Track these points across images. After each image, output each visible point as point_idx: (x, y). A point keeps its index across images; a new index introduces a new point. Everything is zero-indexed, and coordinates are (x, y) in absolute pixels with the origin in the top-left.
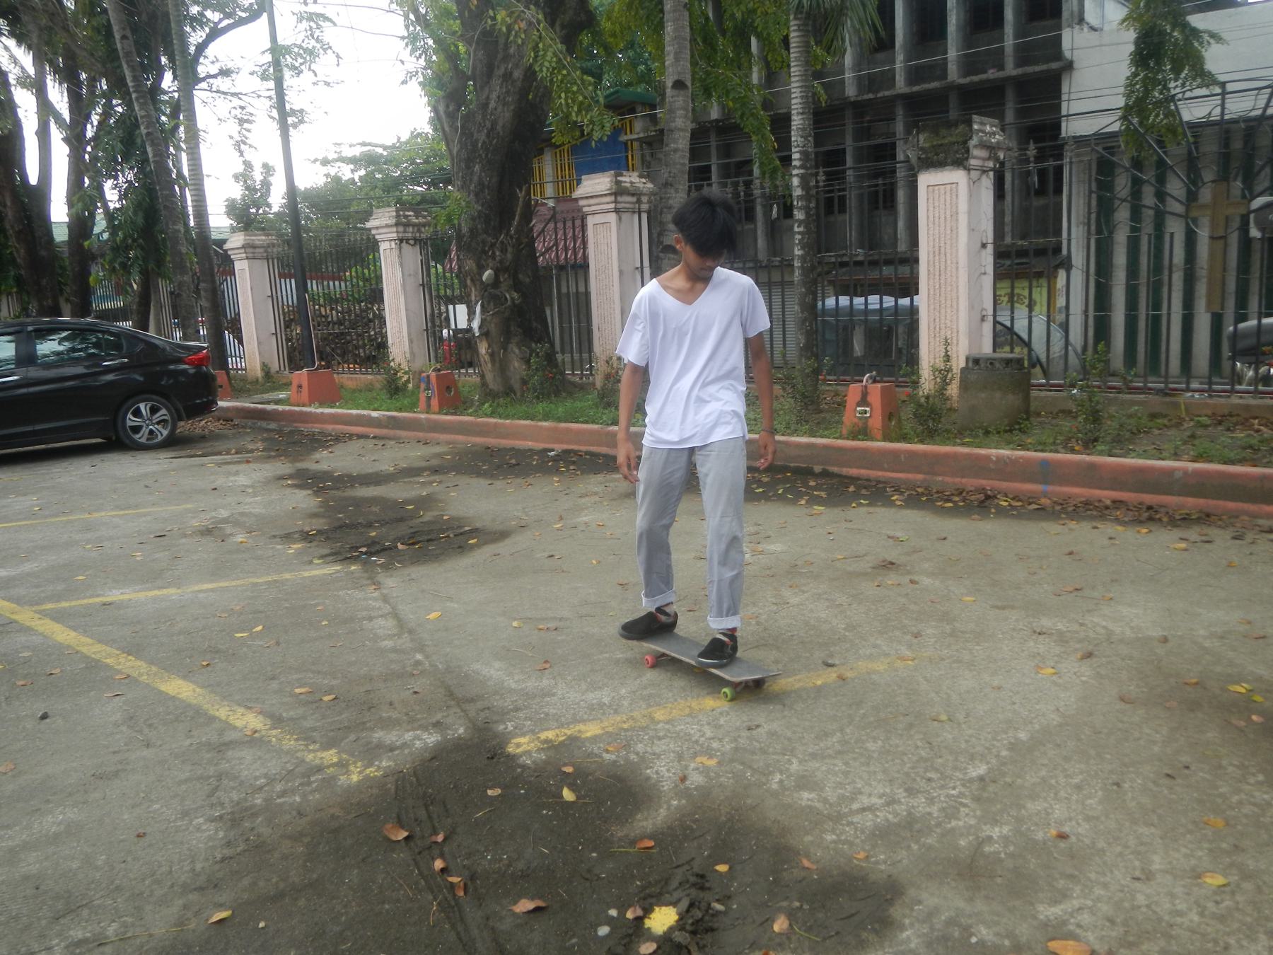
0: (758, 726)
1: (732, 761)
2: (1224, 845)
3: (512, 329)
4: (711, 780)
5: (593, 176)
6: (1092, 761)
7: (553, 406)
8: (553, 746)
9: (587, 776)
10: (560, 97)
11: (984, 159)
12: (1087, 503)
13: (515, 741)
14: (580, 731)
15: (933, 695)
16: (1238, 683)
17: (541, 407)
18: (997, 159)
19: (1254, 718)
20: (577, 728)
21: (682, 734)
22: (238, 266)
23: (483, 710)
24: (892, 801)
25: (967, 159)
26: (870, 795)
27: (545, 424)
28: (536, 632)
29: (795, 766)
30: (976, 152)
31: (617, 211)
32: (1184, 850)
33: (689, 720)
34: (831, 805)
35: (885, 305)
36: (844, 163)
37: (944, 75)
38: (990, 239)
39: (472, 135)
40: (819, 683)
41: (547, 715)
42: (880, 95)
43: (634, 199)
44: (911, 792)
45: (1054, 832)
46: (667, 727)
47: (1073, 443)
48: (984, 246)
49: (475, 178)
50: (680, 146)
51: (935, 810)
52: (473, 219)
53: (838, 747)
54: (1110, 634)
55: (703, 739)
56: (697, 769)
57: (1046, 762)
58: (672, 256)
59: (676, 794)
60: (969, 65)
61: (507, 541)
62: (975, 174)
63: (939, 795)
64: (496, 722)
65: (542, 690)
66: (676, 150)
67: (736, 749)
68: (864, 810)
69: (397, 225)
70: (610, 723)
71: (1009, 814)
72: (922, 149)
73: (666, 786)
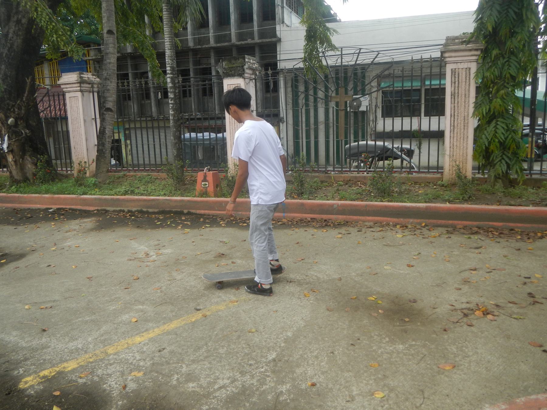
0: (164, 349)
1: (151, 371)
2: (380, 376)
3: (26, 148)
4: (140, 385)
5: (68, 73)
6: (320, 343)
7: (51, 187)
8: (48, 379)
9: (69, 396)
11: (251, 74)
12: (301, 220)
13: (24, 380)
14: (64, 368)
15: (248, 319)
16: (371, 296)
17: (44, 187)
19: (380, 311)
20: (63, 366)
21: (123, 360)
23: (4, 363)
24: (234, 381)
25: (244, 74)
26: (223, 379)
28: (39, 310)
29: (184, 369)
30: (247, 71)
31: (81, 91)
32: (364, 382)
33: (127, 351)
34: (204, 388)
35: (211, 137)
36: (189, 75)
37: (230, 40)
40: (193, 320)
41: (45, 360)
42: (204, 46)
43: (90, 86)
44: (243, 373)
45: (310, 384)
46: (115, 357)
47: (293, 195)
49: (2, 72)
50: (112, 61)
51: (254, 381)
53: (205, 354)
54: (318, 279)
55: (135, 361)
56: (133, 379)
57: (301, 346)
59: (121, 397)
60: (240, 36)
61: (24, 260)
62: (247, 80)
63: (256, 373)
64: (13, 369)
65: (42, 345)
66: (110, 63)
67: (153, 364)
68: (220, 388)
70: (82, 360)
71: (289, 378)
72: (224, 68)
73: (115, 393)
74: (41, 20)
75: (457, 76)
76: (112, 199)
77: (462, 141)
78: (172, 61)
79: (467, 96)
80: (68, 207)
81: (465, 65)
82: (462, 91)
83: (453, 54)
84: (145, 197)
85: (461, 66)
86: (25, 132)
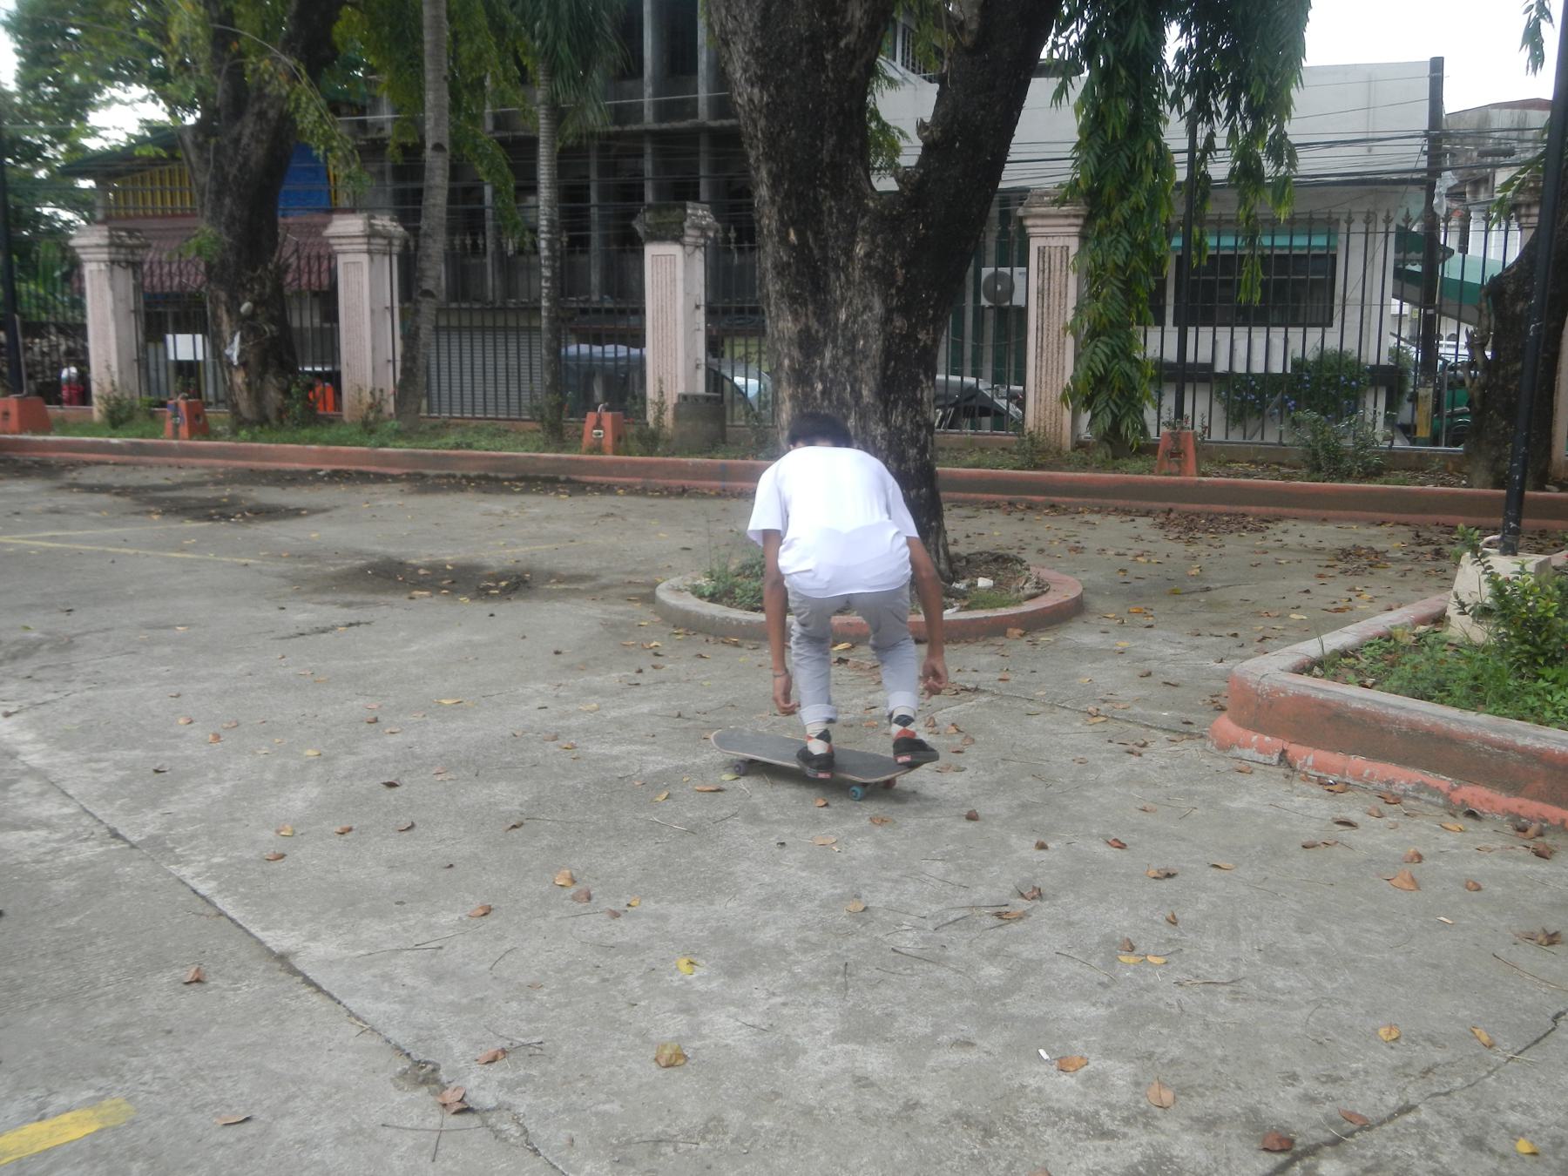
5: (345, 216)
11: (697, 237)
17: (307, 432)
18: (707, 237)
25: (682, 236)
27: (314, 447)
30: (689, 232)
31: (369, 252)
35: (619, 355)
36: (588, 200)
37: (695, 114)
42: (627, 128)
43: (385, 242)
48: (697, 307)
49: (226, 211)
58: (430, 299)
62: (689, 249)
66: (434, 205)
69: (110, 245)
72: (648, 225)
75: (1046, 259)
76: (435, 456)
80: (353, 468)
81: (1060, 242)
82: (1055, 287)
83: (1039, 222)
84: (494, 453)
85: (1053, 242)
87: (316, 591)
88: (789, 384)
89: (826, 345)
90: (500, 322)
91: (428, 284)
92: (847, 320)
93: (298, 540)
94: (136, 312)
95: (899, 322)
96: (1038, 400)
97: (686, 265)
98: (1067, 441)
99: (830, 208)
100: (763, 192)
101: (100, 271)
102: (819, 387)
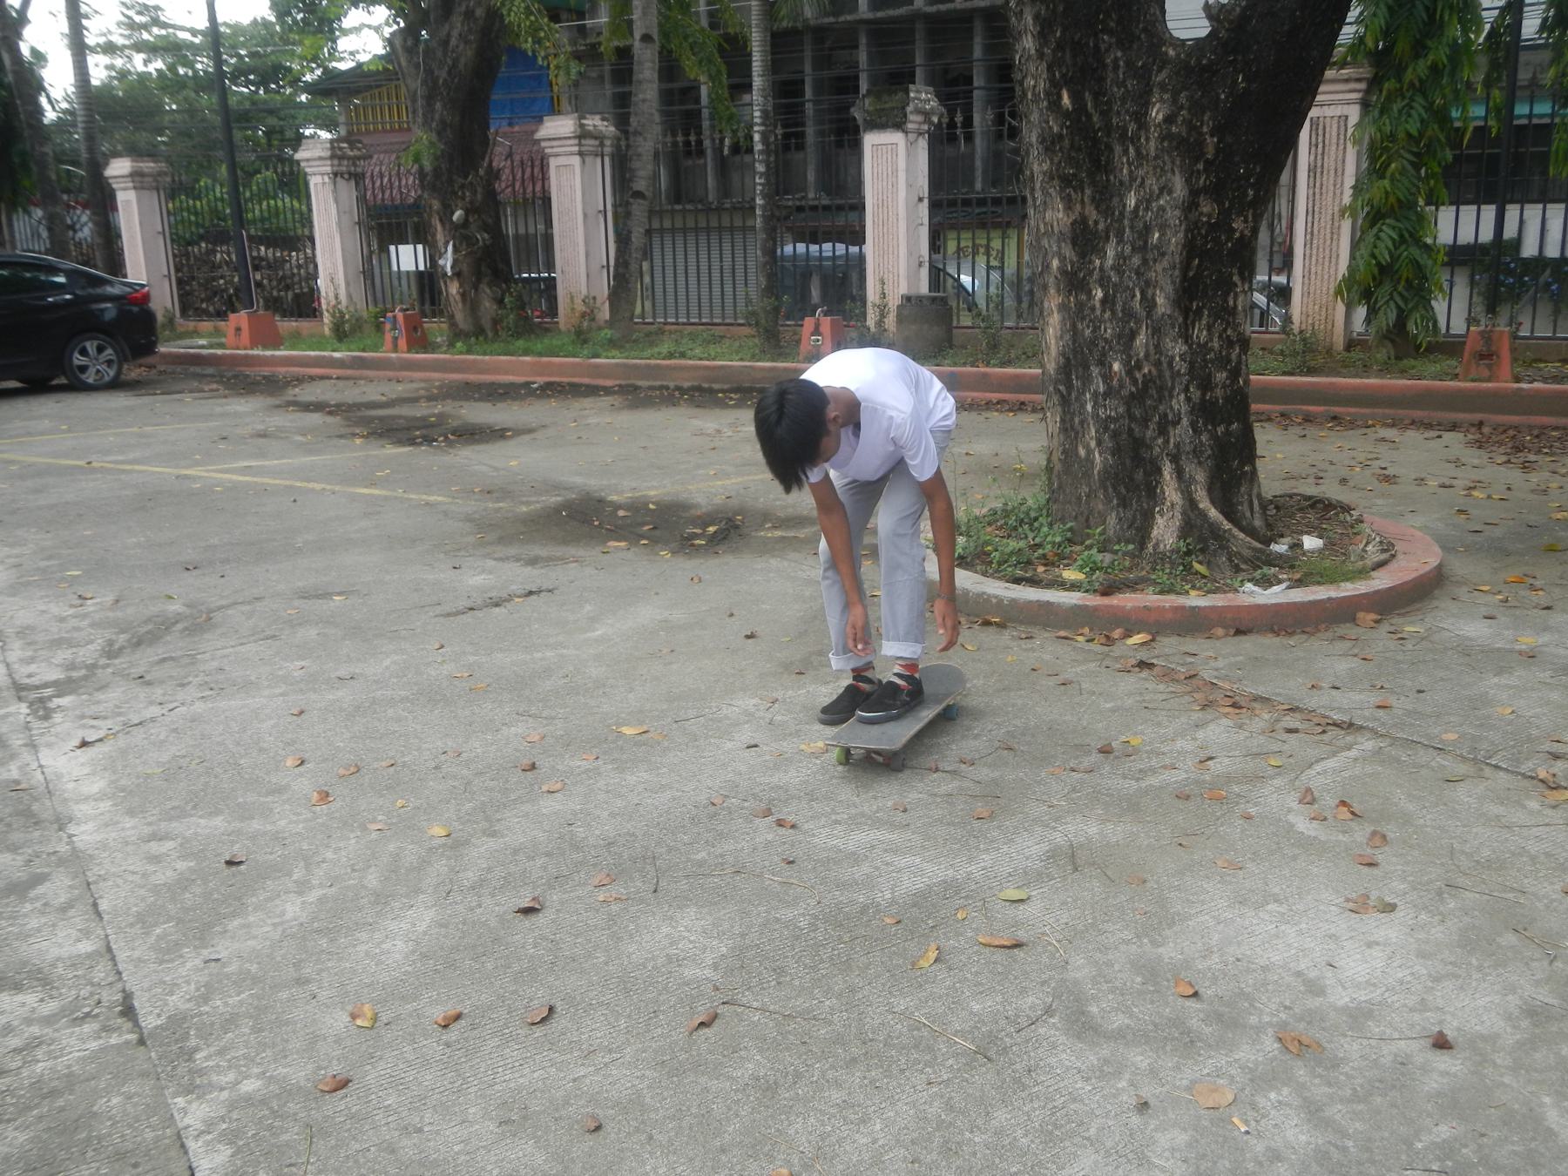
3: (483, 269)
10: (526, 41)
11: (920, 123)
17: (520, 343)
18: (931, 123)
22: (121, 197)
25: (905, 123)
27: (527, 359)
30: (912, 117)
31: (581, 154)
35: (837, 253)
36: (803, 95)
38: (926, 195)
39: (433, 73)
42: (842, 19)
43: (597, 143)
48: (921, 200)
49: (437, 116)
50: (648, 97)
52: (436, 158)
58: (641, 201)
62: (912, 136)
66: (644, 101)
69: (332, 157)
74: (510, 10)
75: (1320, 132)
76: (648, 366)
77: (1327, 264)
78: (765, 98)
79: (1339, 173)
80: (565, 380)
82: (1330, 162)
84: (707, 363)
86: (482, 237)
87: (501, 540)
88: (1058, 291)
89: (1108, 238)
90: (667, 224)
91: (640, 185)
92: (1137, 207)
93: (496, 469)
94: (359, 223)
95: (1207, 207)
96: (1306, 294)
97: (908, 155)
98: (1339, 341)
99: (1116, 60)
100: (1028, 43)
101: (324, 184)
102: (1099, 294)
